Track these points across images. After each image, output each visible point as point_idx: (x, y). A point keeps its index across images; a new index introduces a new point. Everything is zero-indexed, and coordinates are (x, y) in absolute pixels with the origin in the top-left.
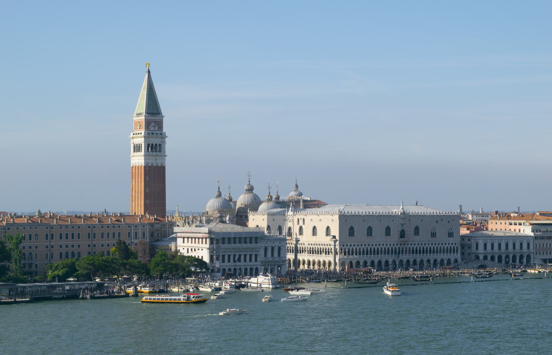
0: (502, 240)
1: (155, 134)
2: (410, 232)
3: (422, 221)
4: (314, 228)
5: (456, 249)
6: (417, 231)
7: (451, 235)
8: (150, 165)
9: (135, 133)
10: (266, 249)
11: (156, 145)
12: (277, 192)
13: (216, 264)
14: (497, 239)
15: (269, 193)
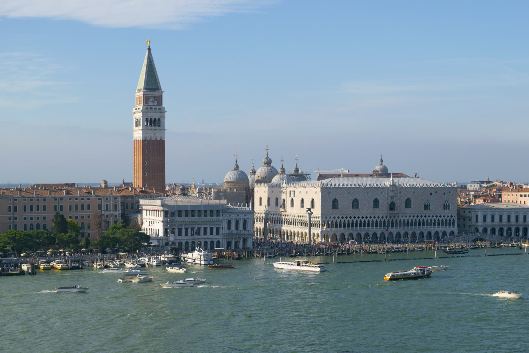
0: (503, 213)
1: (153, 109)
2: (400, 204)
3: (414, 193)
4: (302, 200)
5: (452, 221)
6: (408, 203)
7: (446, 207)
8: (148, 139)
9: (136, 108)
10: (229, 222)
11: (155, 119)
12: (297, 165)
13: (170, 237)
14: (498, 211)
15: (282, 166)
